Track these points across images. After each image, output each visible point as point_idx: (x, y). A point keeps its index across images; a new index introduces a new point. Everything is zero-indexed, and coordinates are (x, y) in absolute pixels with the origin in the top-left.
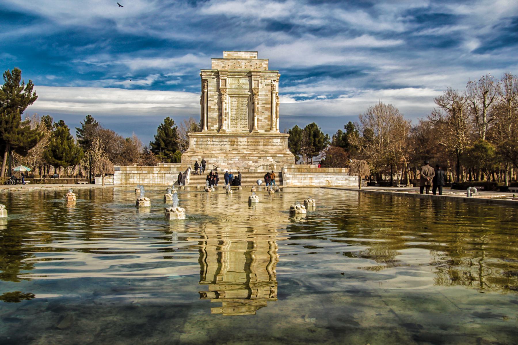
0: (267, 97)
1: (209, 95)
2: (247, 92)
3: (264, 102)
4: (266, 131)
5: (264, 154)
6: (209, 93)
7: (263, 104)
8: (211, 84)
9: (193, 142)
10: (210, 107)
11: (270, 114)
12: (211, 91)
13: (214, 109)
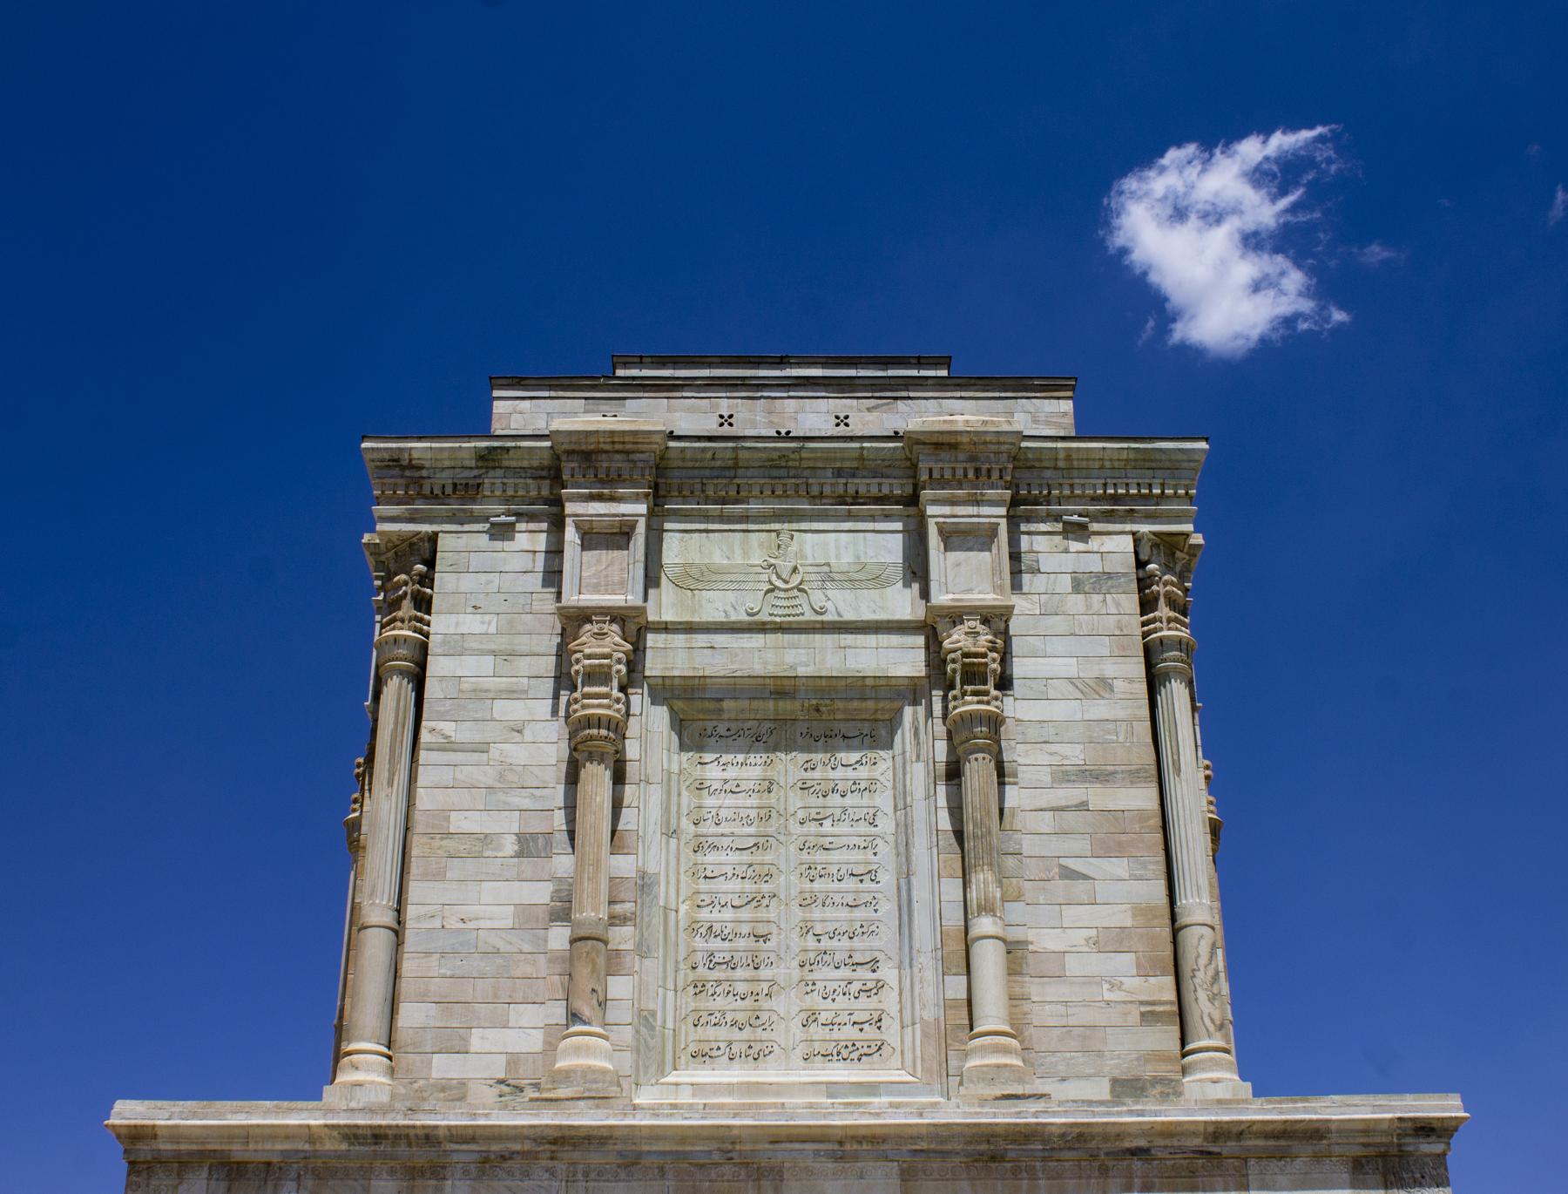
0: (1100, 709)
1: (432, 689)
3: (1074, 754)
4: (1126, 1088)
6: (435, 666)
7: (1064, 776)
8: (467, 583)
10: (444, 814)
11: (1160, 886)
12: (458, 647)
13: (486, 838)
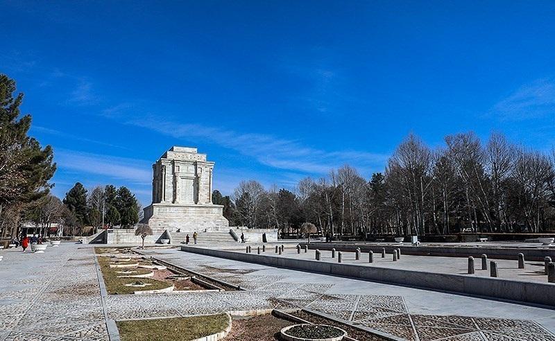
2: (193, 175)
5: (207, 219)
9: (156, 210)
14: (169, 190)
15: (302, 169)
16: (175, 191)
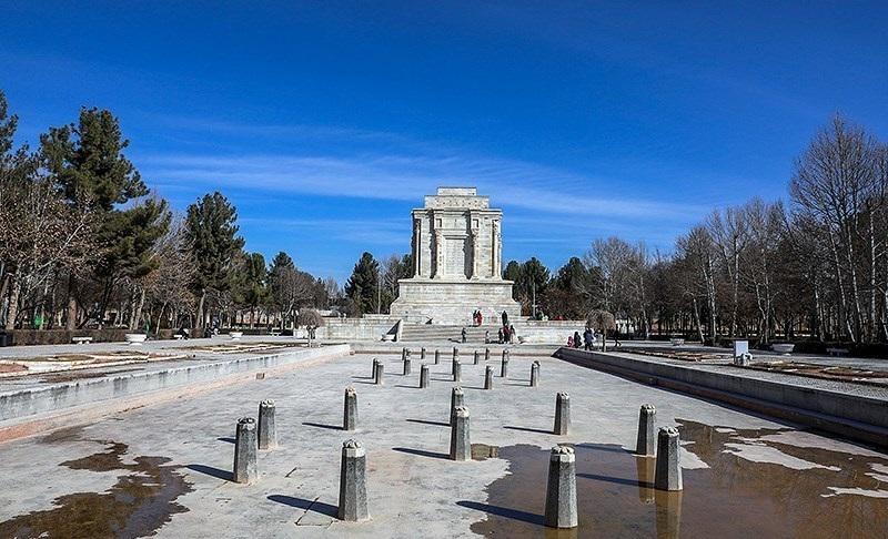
2: (464, 233)
5: (484, 304)
9: (403, 289)
14: (426, 258)
15: (646, 221)
16: (434, 259)
